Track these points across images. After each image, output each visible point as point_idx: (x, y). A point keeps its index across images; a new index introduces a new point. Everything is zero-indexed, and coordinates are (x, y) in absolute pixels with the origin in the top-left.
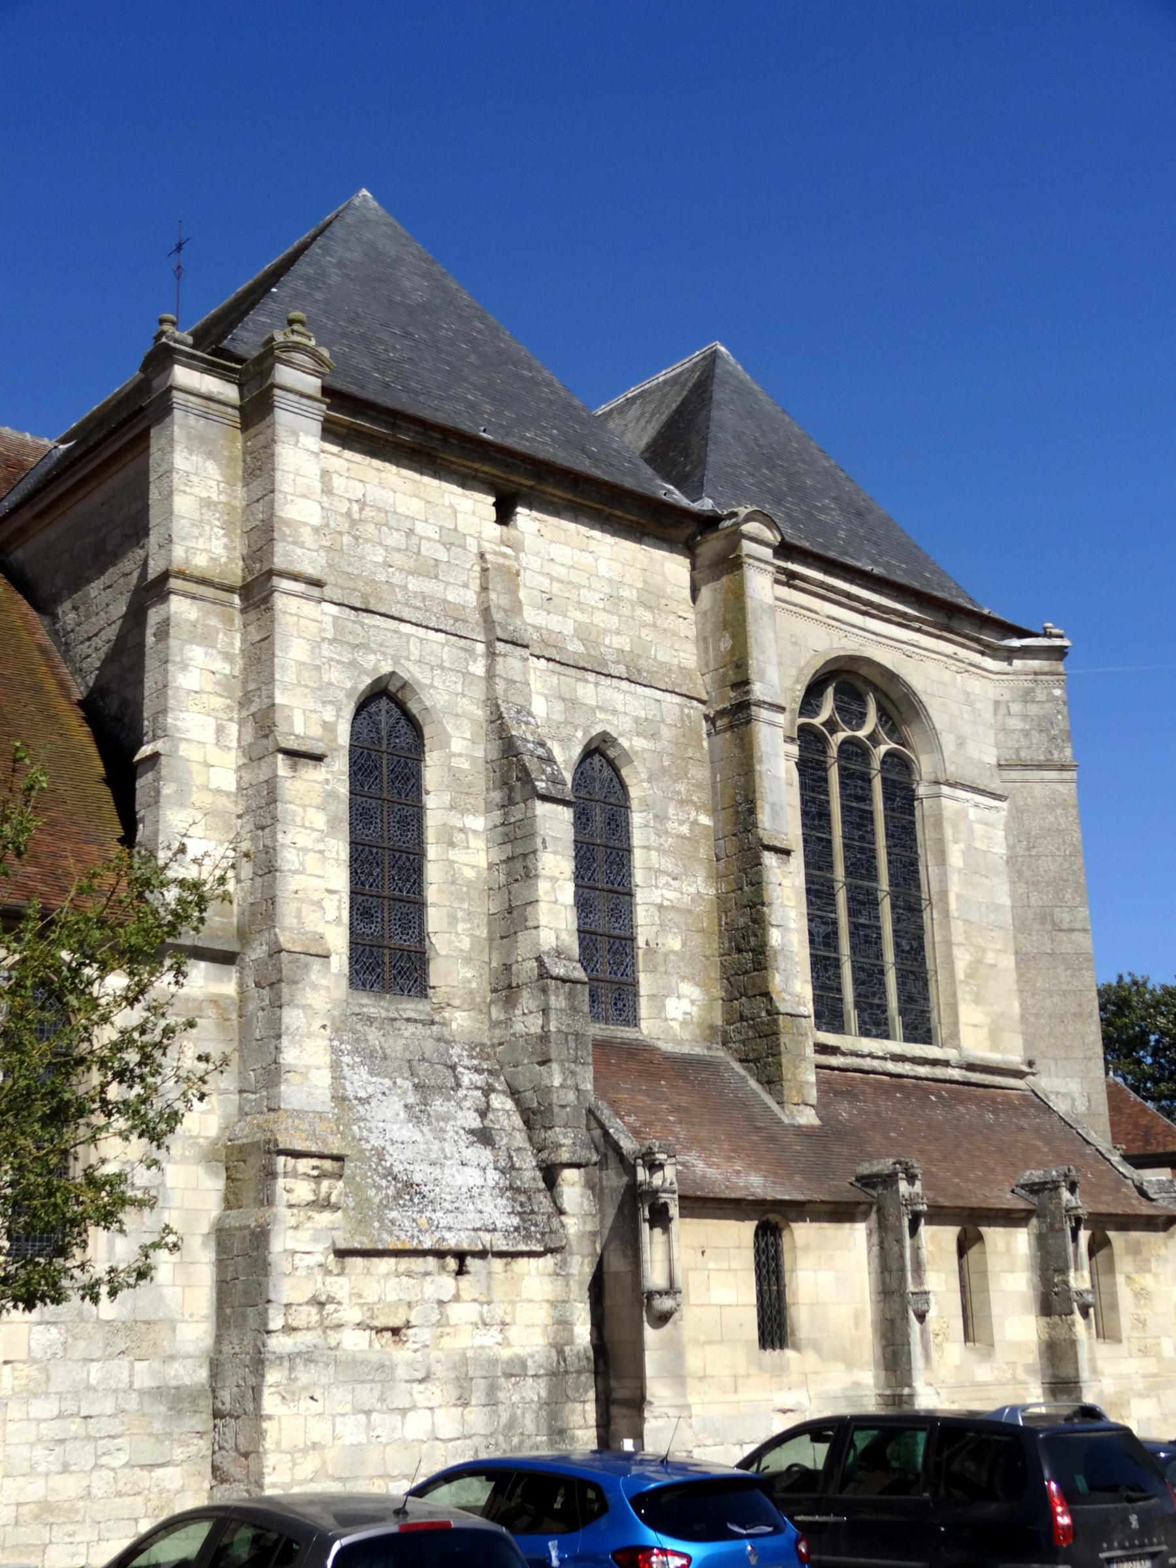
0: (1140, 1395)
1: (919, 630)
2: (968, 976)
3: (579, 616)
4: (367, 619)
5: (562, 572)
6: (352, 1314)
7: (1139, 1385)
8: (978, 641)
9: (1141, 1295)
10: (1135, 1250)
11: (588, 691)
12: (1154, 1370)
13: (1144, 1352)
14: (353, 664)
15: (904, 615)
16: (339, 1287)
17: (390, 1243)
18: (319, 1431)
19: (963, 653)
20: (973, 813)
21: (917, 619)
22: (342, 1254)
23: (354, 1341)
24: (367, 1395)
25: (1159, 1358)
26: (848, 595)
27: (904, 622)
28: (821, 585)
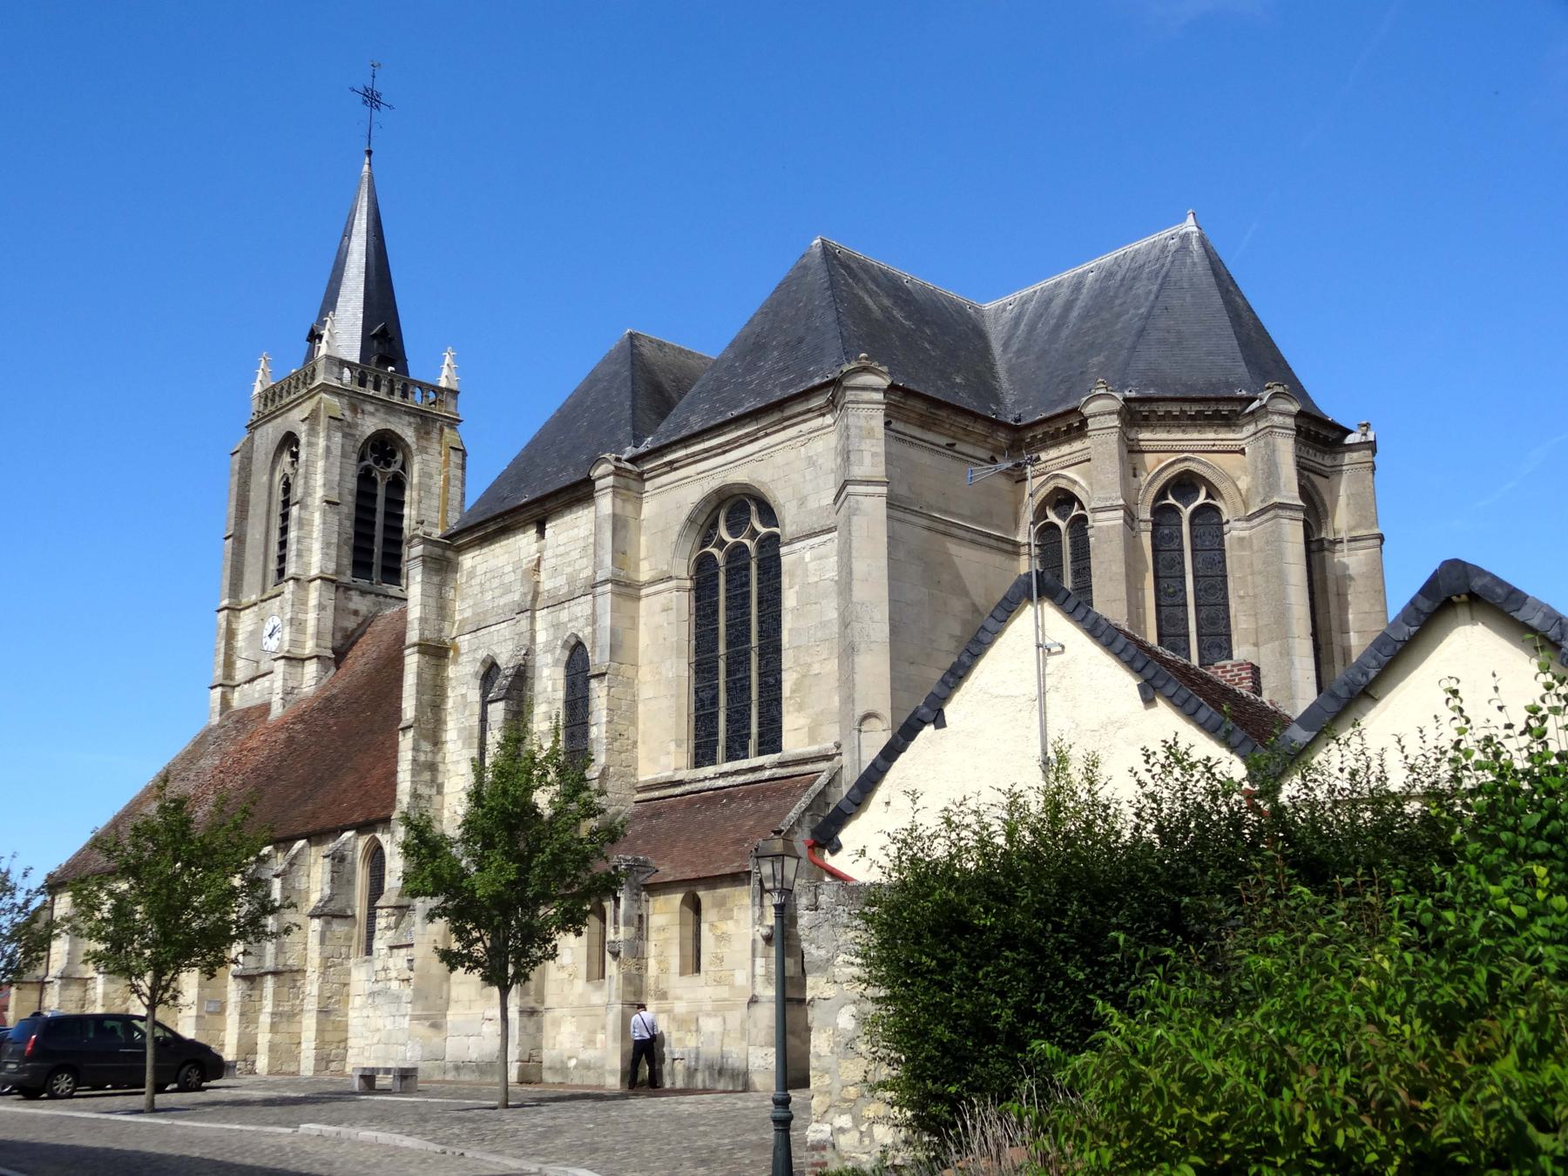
0: (708, 1015)
1: (767, 435)
2: (793, 691)
3: (569, 570)
4: (479, 633)
5: (561, 550)
6: (393, 974)
7: (708, 1007)
8: (810, 411)
9: (722, 938)
10: (720, 904)
11: (564, 615)
12: (726, 995)
13: (719, 982)
14: (474, 659)
15: (747, 435)
16: (391, 963)
17: (404, 942)
18: (380, 1023)
19: (804, 427)
20: (808, 557)
21: (759, 430)
22: (391, 948)
23: (394, 985)
24: (393, 1008)
25: (732, 986)
26: (706, 451)
27: (753, 438)
28: (687, 456)
